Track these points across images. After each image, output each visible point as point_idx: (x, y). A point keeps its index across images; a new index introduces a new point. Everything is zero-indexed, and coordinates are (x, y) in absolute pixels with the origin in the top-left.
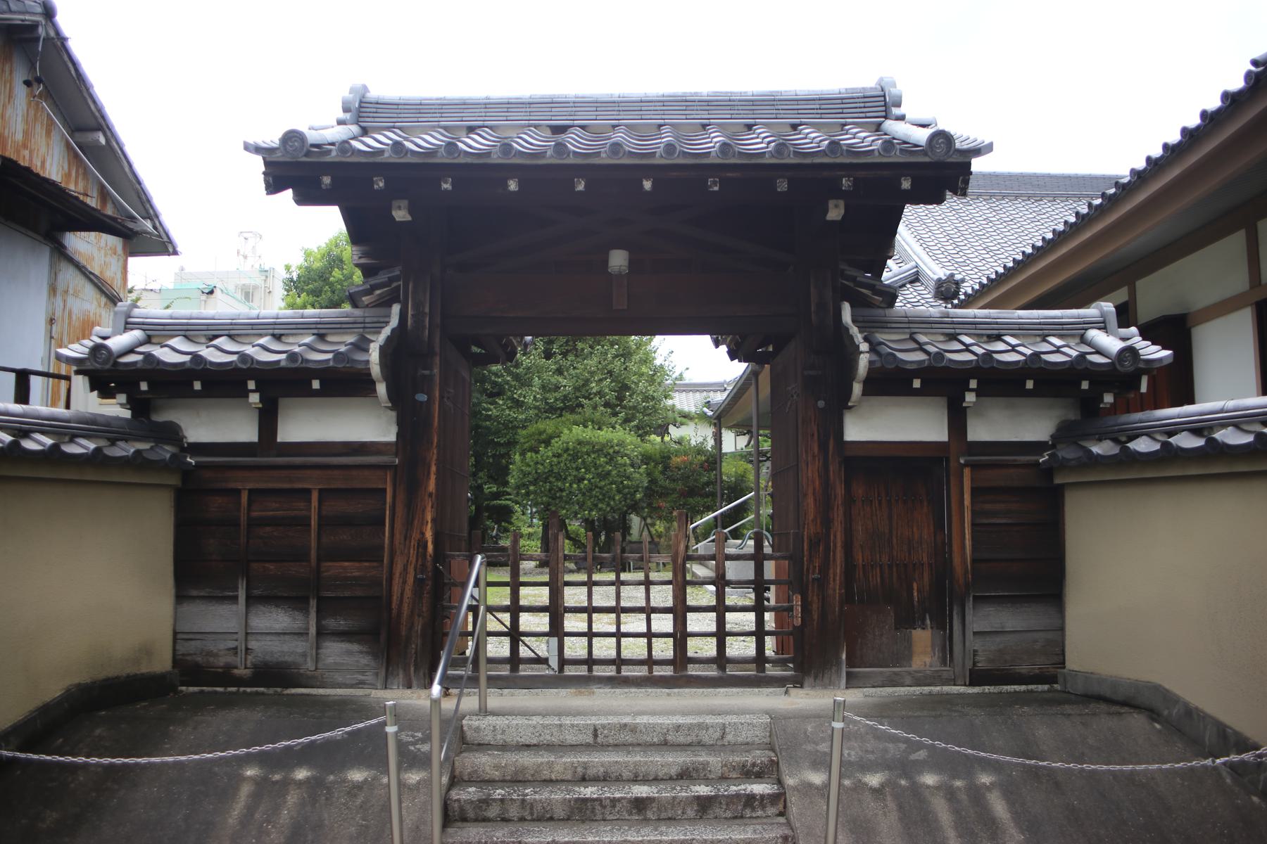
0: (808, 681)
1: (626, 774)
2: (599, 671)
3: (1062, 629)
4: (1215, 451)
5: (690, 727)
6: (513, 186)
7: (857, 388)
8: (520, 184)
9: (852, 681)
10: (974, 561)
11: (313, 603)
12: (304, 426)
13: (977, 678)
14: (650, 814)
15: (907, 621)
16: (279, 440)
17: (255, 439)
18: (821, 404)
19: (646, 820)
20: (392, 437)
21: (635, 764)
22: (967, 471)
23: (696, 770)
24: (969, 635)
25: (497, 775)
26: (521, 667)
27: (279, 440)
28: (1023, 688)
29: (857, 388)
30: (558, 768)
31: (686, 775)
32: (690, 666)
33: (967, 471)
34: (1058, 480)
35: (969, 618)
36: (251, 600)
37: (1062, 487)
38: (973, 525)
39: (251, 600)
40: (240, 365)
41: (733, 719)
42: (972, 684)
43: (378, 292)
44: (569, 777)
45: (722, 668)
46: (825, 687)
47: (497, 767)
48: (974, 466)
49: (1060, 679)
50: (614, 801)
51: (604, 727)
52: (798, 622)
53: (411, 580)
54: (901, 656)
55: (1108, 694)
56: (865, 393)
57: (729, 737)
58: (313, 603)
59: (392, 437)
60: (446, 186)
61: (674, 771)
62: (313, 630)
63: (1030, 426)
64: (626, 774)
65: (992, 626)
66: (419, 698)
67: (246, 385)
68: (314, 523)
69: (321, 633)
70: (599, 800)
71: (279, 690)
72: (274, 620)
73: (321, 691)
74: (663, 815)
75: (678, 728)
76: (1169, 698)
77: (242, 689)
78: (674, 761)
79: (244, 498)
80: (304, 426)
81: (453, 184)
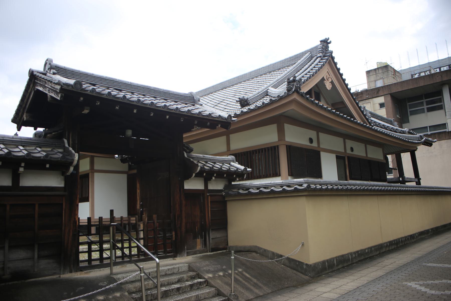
0: (178, 255)
1: (166, 283)
2: (126, 259)
3: (227, 236)
4: (261, 193)
5: (171, 269)
6: (135, 111)
7: (194, 175)
8: (137, 111)
9: (188, 254)
10: (211, 220)
11: (36, 247)
12: (30, 181)
13: (213, 250)
14: (181, 292)
15: (195, 237)
16: (20, 185)
17: (203, 188)
18: (180, 179)
19: (180, 294)
20: (62, 185)
21: (168, 280)
22: (209, 197)
23: (181, 279)
24: (211, 239)
25: (134, 290)
26: (104, 261)
27: (20, 185)
28: (221, 251)
29: (194, 175)
30: (150, 285)
31: (179, 281)
32: (104, 261)
33: (209, 197)
34: (226, 199)
35: (211, 235)
36: (10, 247)
37: (226, 201)
38: (211, 211)
39: (10, 247)
40: (26, 157)
41: (181, 265)
42: (212, 252)
43: (53, 133)
44: (153, 287)
45: (123, 259)
46: (182, 256)
47: (135, 288)
48: (211, 196)
49: (228, 248)
50: (173, 289)
51: (151, 272)
52: (174, 239)
53: (71, 234)
54: (195, 247)
55: (243, 250)
56: (195, 176)
57: (180, 270)
58: (36, 247)
59: (62, 185)
60: (117, 108)
61: (176, 280)
62: (36, 256)
63: (217, 185)
64: (166, 283)
65: (214, 235)
66: (77, 275)
67: (21, 164)
68: (36, 216)
69: (39, 257)
70: (169, 290)
71: (23, 281)
72: (21, 254)
73: (40, 279)
74: (183, 291)
75: (169, 269)
76: (260, 248)
77: (7, 283)
78: (175, 278)
79: (8, 208)
80: (30, 181)
81: (119, 108)
